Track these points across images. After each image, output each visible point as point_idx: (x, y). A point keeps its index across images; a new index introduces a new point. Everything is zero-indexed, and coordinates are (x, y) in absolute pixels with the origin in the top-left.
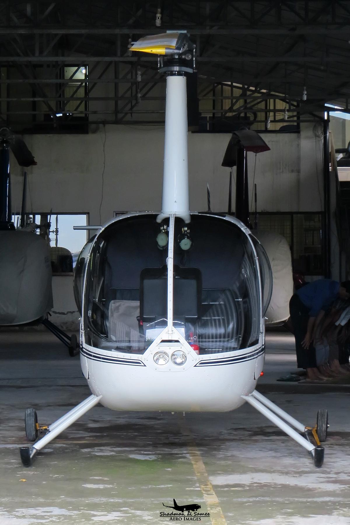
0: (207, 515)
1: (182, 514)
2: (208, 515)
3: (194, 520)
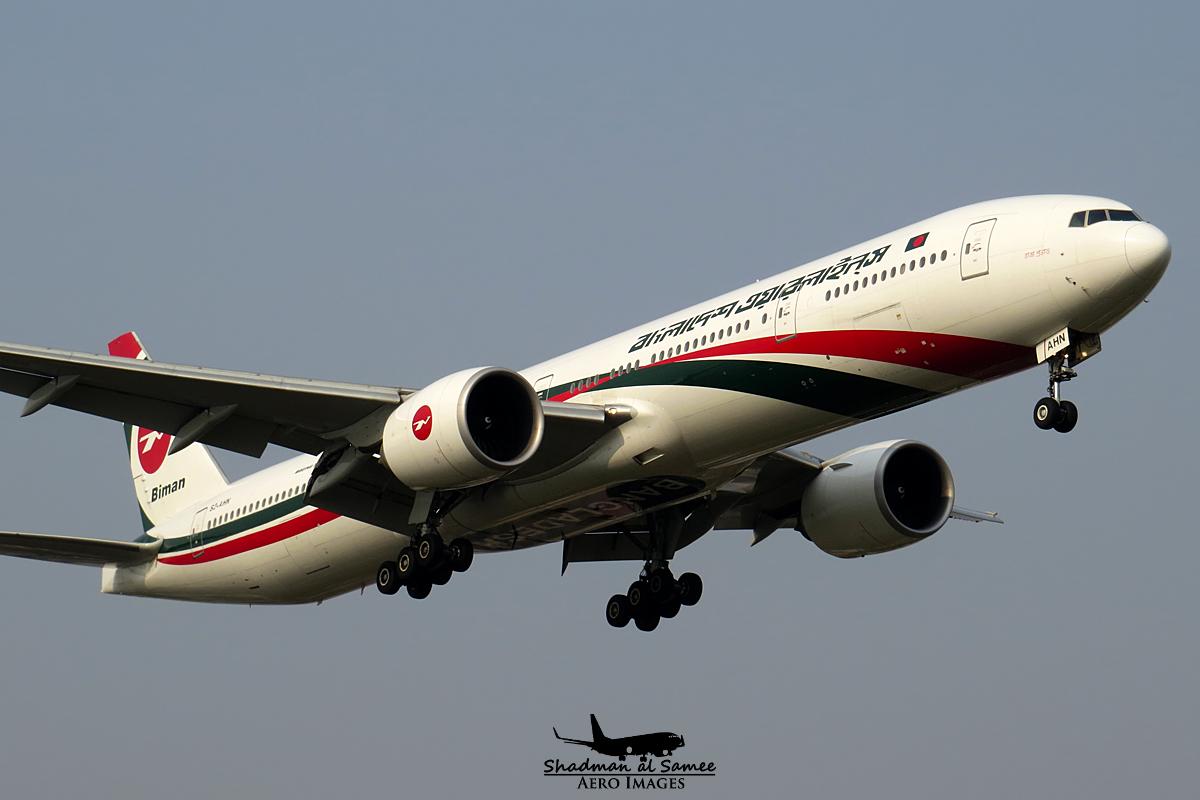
0: (707, 769)
1: (621, 767)
2: (709, 769)
3: (663, 786)
